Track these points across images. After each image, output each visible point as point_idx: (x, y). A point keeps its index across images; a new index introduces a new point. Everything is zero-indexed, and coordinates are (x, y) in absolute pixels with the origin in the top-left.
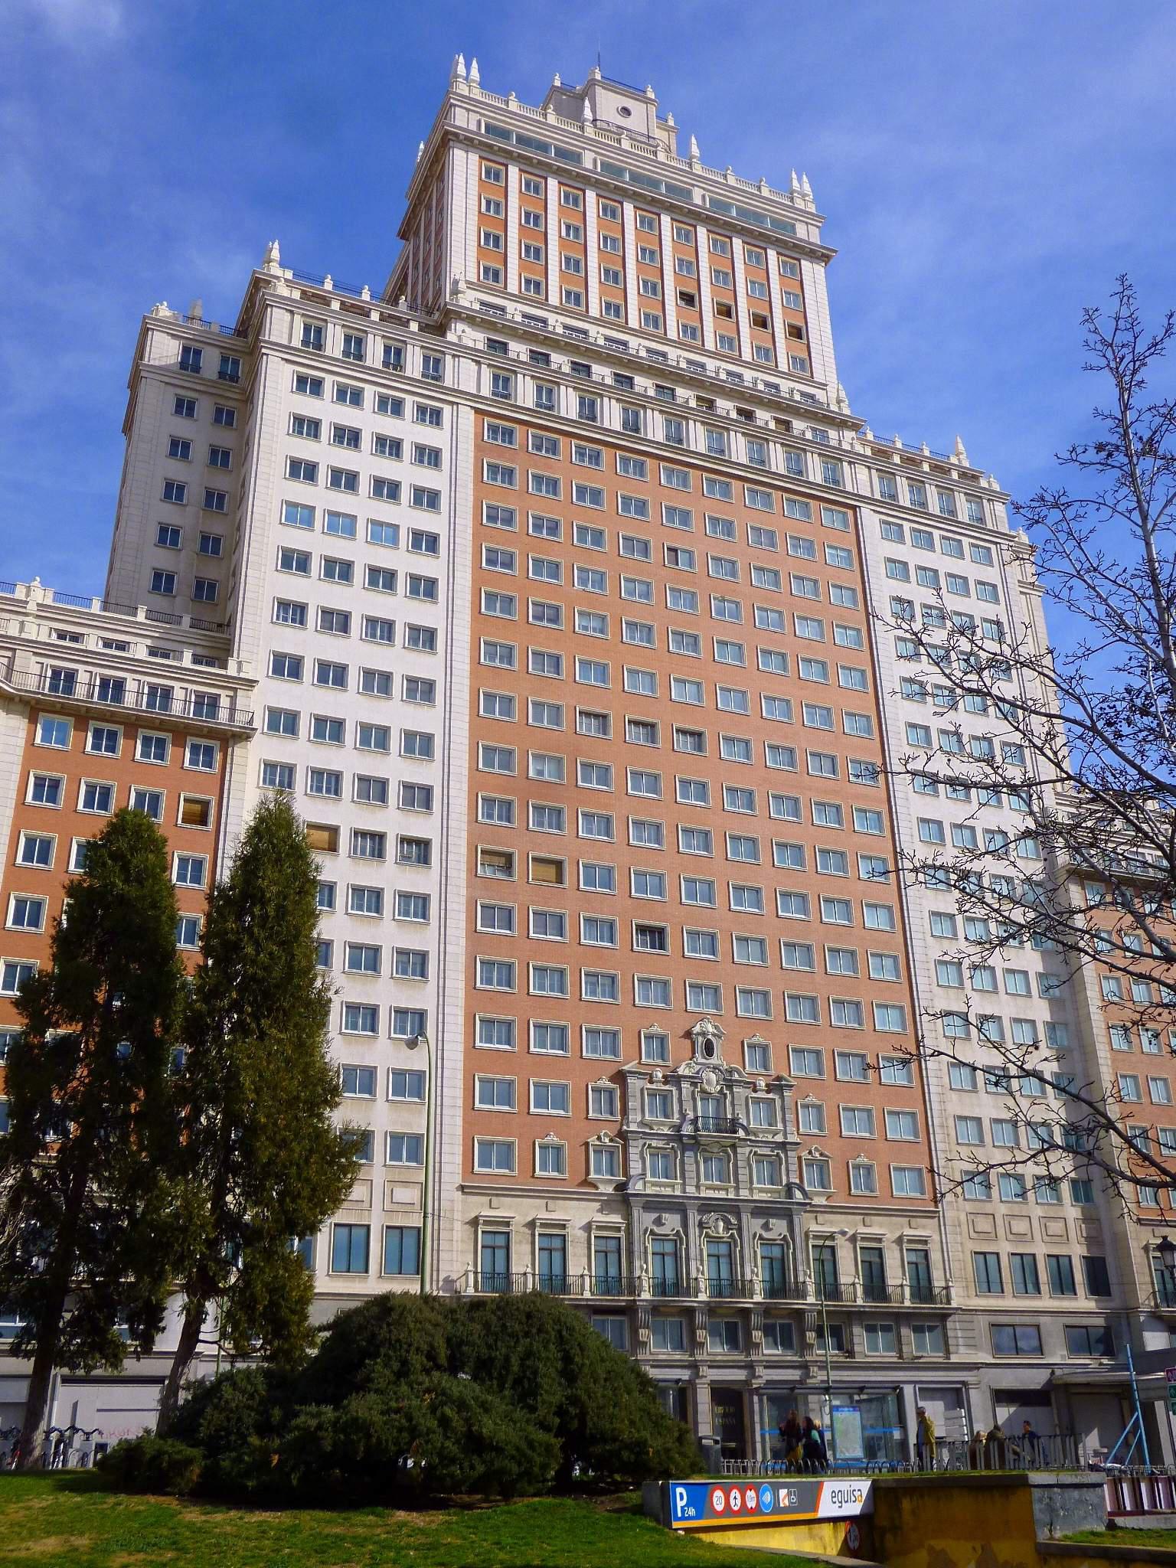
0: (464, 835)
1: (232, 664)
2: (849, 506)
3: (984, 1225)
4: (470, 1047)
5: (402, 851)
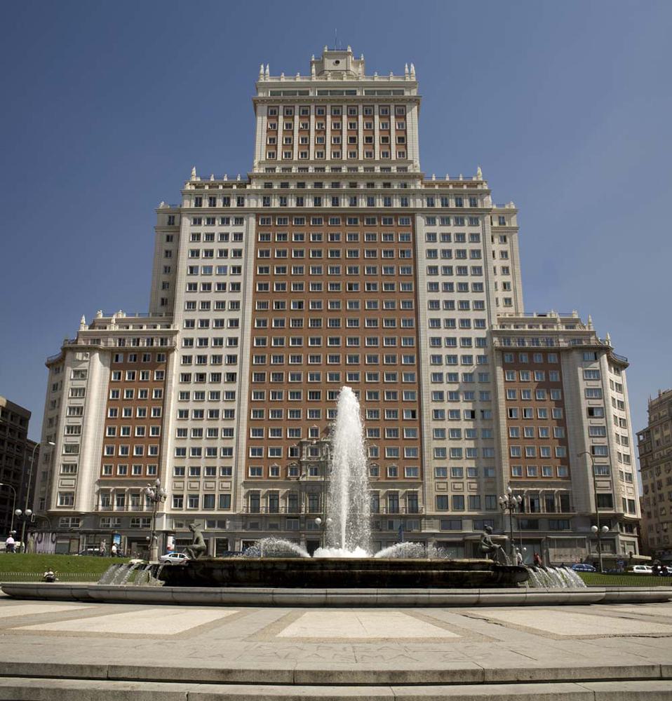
1: (172, 326)
2: (411, 215)
3: (442, 486)
4: (249, 439)
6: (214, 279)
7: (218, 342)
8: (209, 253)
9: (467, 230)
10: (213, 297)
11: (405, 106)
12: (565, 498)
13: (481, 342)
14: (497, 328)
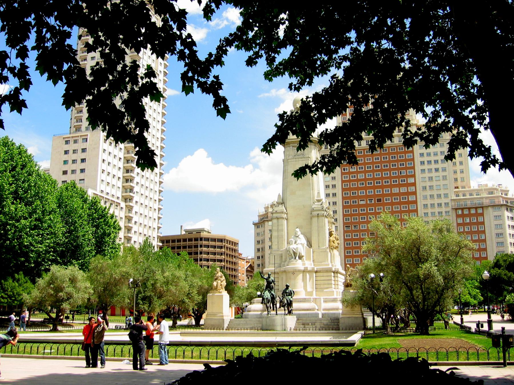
13: (447, 204)
14: (454, 197)
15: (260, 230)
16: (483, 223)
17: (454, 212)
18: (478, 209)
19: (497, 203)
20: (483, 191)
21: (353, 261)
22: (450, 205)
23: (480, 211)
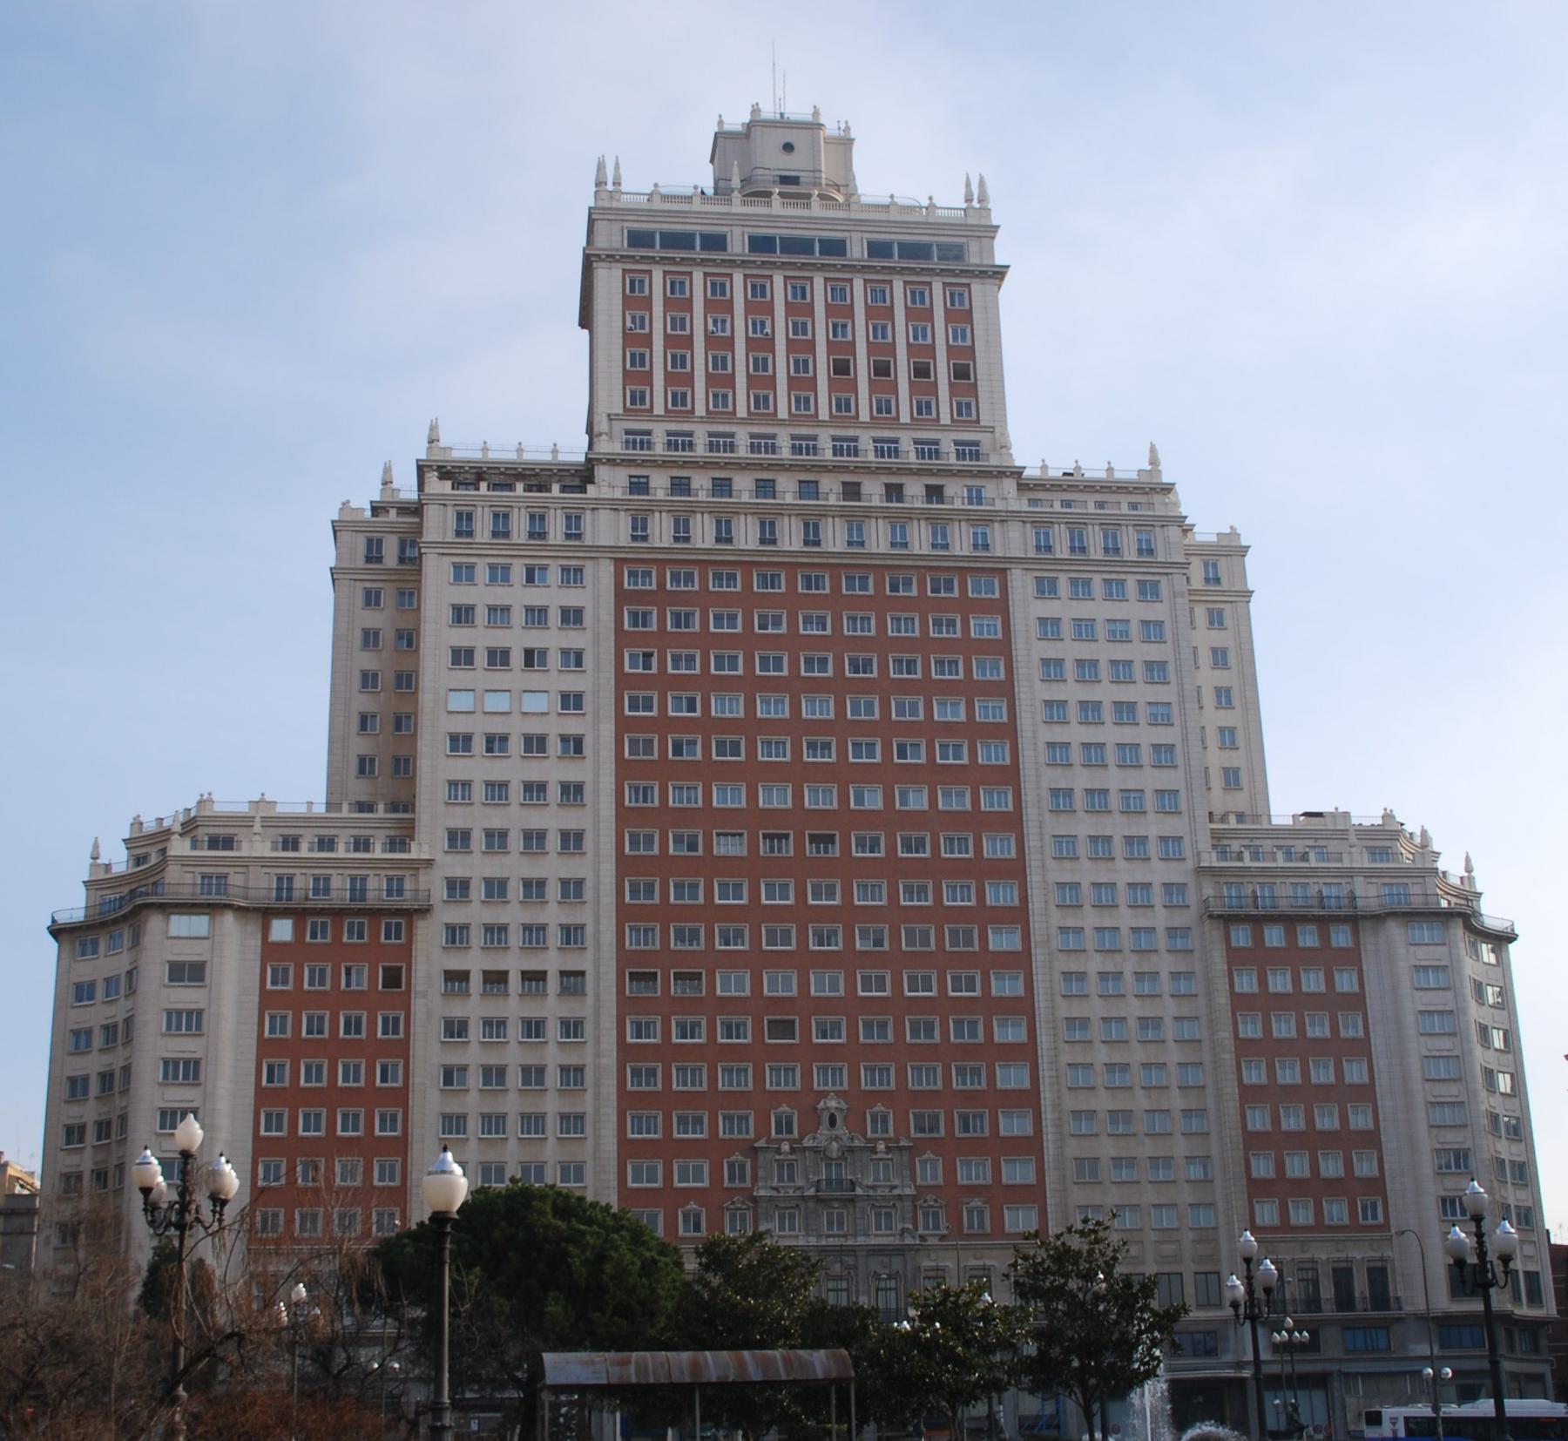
0: (614, 963)
1: (414, 846)
5: (562, 983)
6: (516, 730)
7: (534, 888)
8: (499, 657)
9: (1134, 610)
10: (515, 769)
11: (968, 285)
12: (1379, 1275)
14: (1211, 860)
15: (107, 963)
16: (1357, 1002)
17: (1215, 933)
18: (1333, 929)
19: (1417, 902)
20: (1353, 839)
21: (668, 1176)
22: (1192, 898)
23: (1341, 937)
